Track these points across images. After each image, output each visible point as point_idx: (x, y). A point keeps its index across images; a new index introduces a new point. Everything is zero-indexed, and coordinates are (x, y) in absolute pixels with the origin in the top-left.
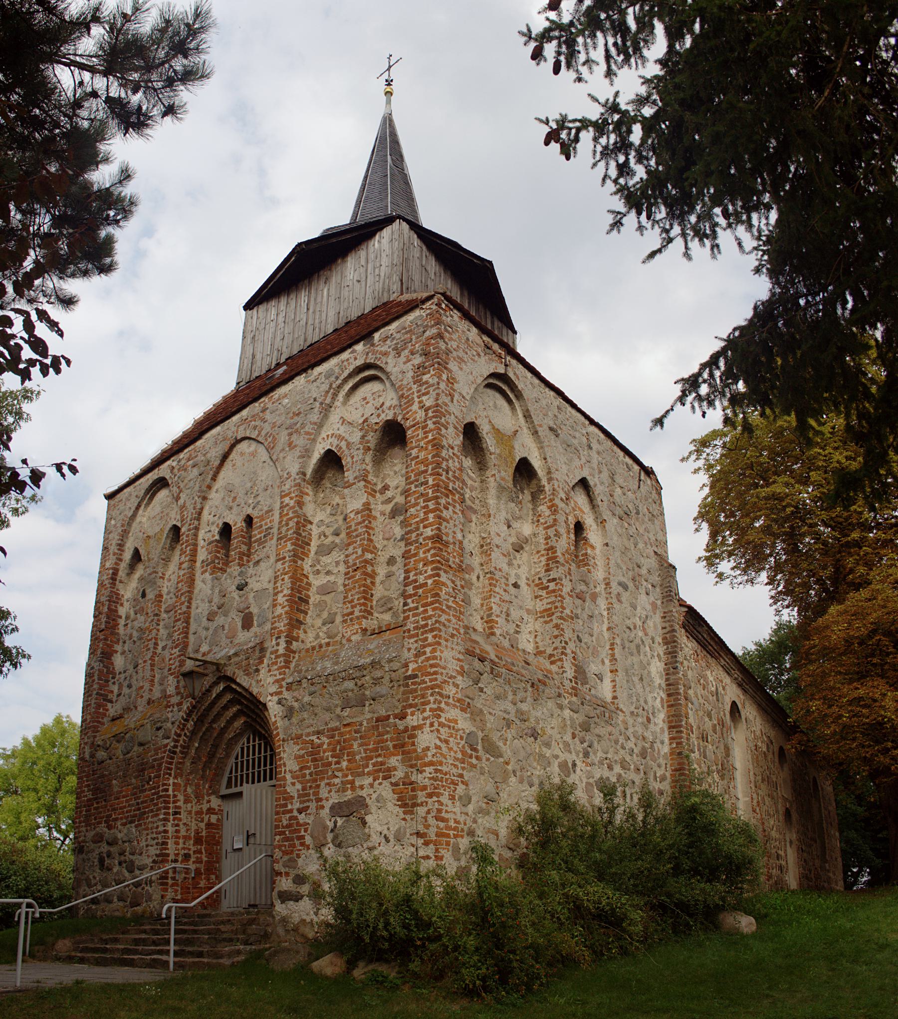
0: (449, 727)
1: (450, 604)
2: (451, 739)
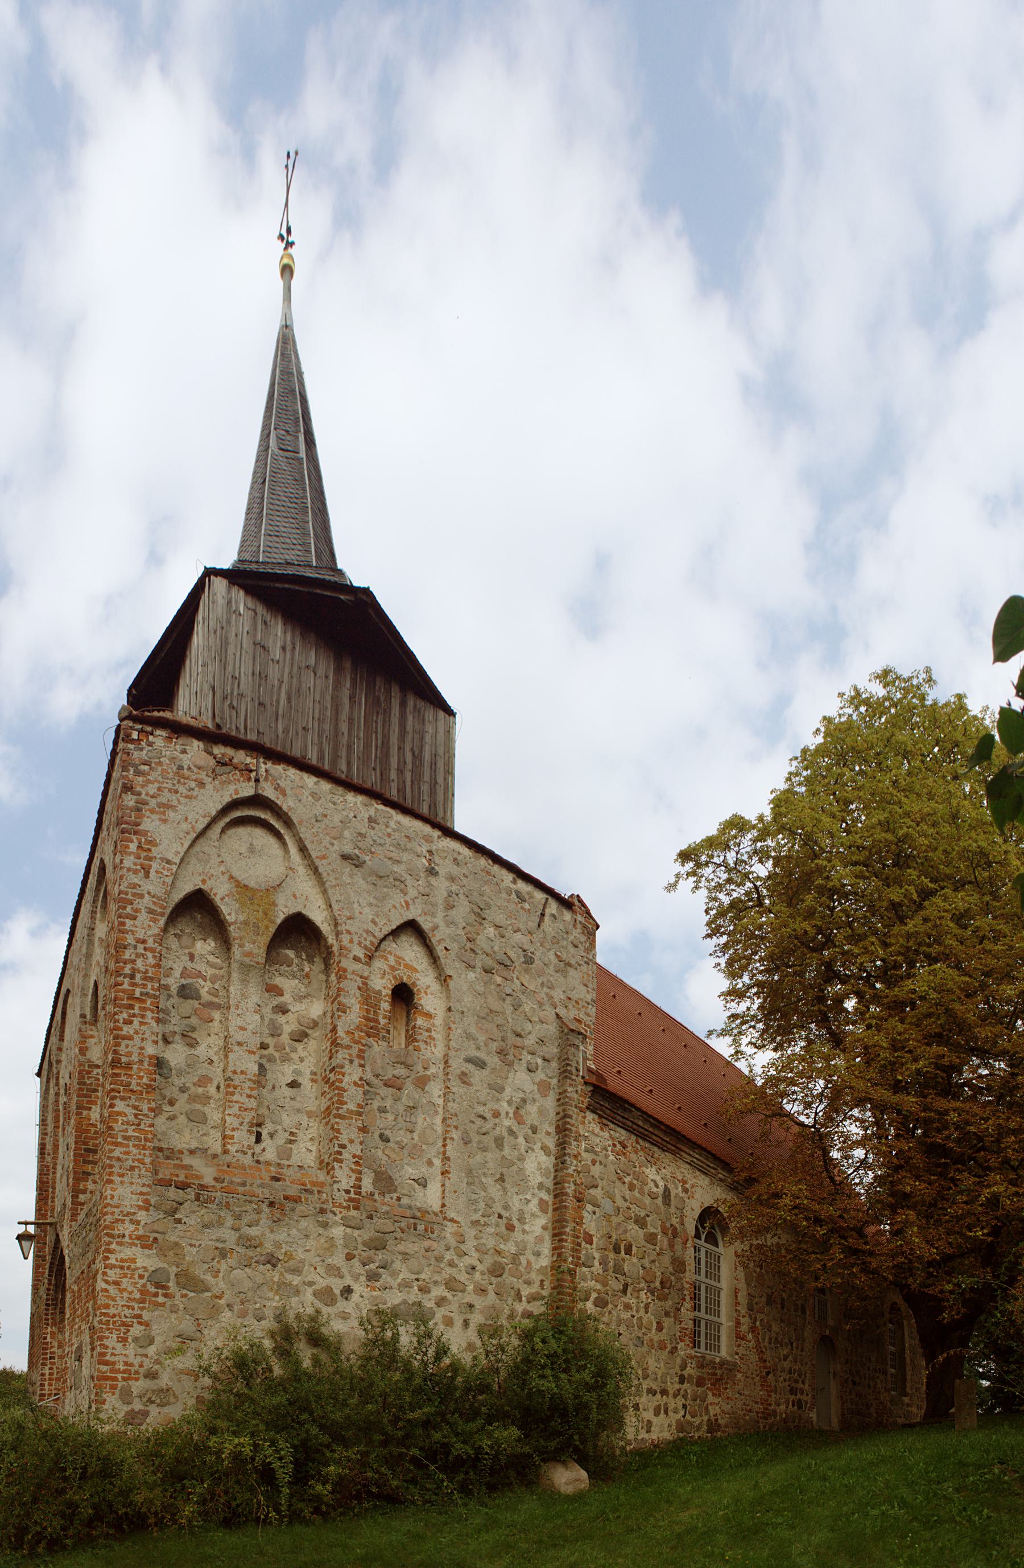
0: (122, 1268)
1: (130, 1133)
2: (124, 1280)
